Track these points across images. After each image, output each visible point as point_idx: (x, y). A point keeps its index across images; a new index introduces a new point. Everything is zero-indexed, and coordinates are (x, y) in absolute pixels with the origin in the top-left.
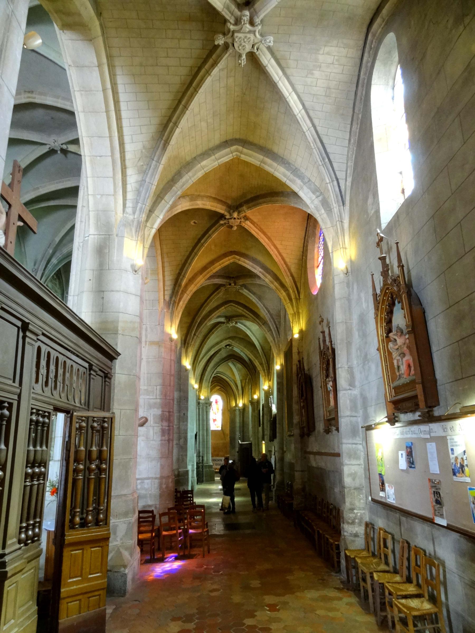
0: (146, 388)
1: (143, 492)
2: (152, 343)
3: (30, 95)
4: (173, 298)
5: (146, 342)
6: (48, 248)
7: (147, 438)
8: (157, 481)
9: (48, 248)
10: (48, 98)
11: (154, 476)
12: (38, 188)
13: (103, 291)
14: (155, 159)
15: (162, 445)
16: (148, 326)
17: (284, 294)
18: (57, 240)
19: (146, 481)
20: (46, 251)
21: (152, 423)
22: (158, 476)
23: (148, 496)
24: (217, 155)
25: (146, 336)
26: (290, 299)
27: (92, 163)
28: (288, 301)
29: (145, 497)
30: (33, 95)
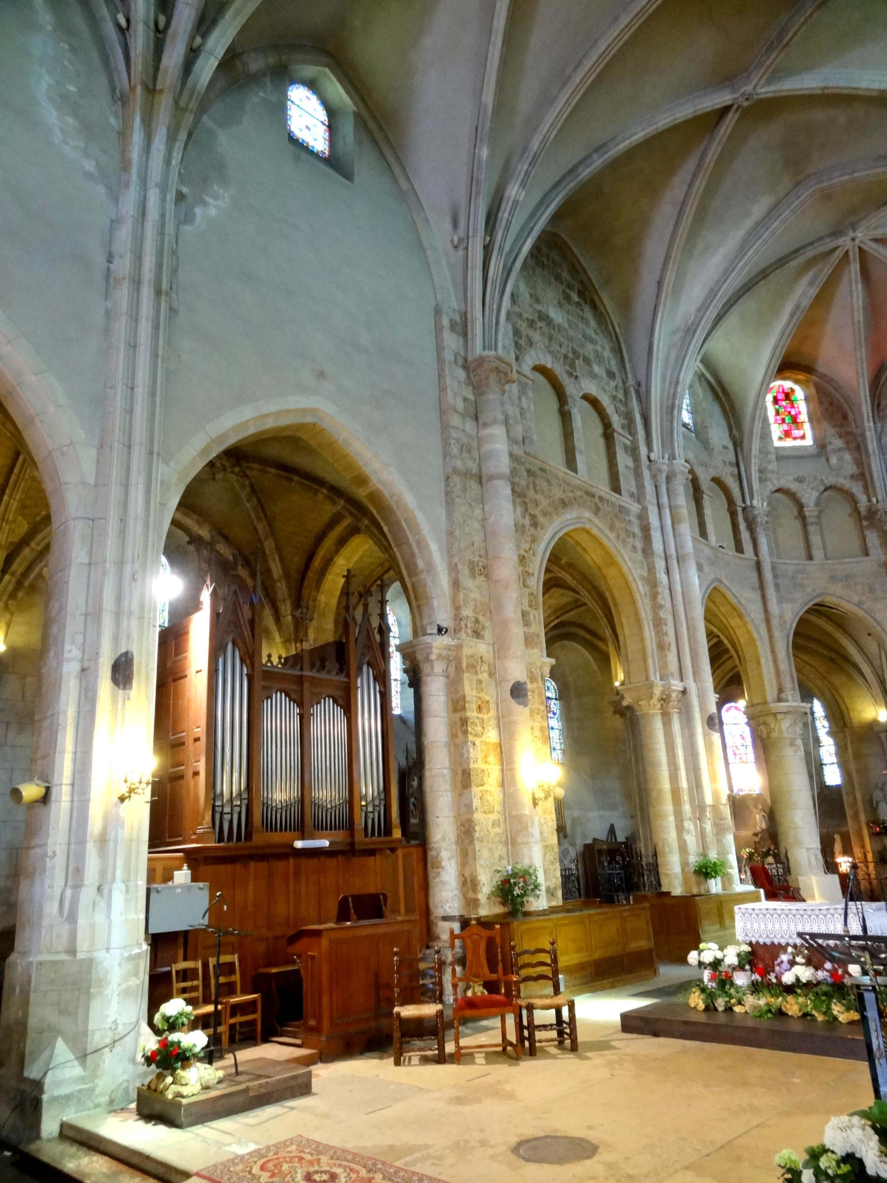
18: (489, 97)
20: (474, 157)
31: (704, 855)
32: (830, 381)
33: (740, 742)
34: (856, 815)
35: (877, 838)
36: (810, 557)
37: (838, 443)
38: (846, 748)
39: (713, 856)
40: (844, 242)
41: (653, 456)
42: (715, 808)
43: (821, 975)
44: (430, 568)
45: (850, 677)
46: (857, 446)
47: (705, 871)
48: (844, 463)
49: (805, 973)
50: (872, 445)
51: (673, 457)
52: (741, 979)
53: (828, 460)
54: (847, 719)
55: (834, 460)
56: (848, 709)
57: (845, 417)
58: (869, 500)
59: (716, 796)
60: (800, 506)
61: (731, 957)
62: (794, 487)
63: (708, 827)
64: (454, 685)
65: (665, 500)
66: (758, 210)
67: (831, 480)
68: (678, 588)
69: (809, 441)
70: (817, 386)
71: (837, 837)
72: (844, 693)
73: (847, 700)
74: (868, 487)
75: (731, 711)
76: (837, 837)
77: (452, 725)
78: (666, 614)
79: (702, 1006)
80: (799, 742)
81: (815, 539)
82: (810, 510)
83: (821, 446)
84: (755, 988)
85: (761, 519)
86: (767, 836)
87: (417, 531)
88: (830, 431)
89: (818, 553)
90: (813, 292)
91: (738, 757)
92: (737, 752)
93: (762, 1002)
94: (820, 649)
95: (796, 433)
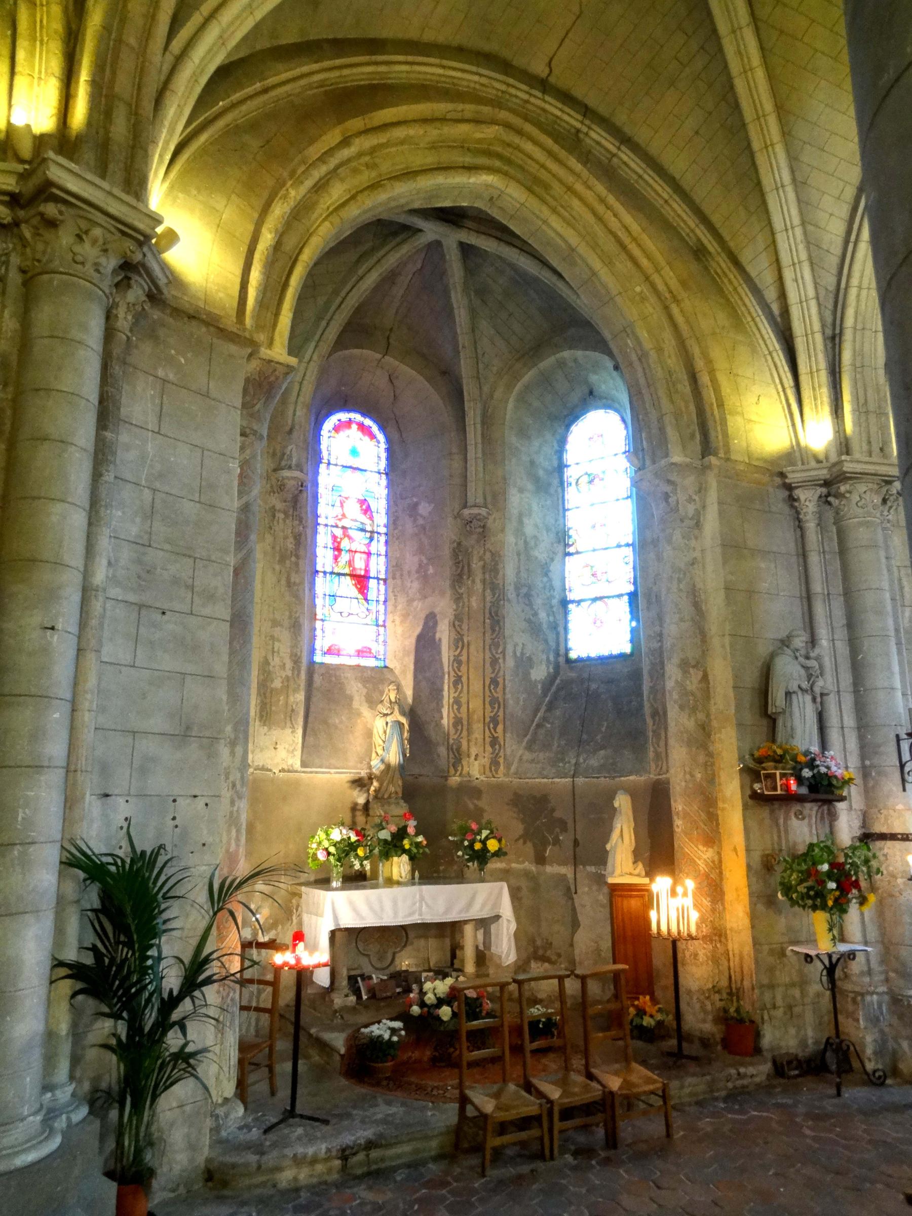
33: (353, 511)
34: (702, 738)
35: (764, 812)
38: (698, 525)
45: (737, 322)
54: (716, 436)
56: (721, 405)
71: (622, 802)
72: (716, 353)
73: (722, 378)
75: (343, 434)
76: (622, 802)
86: (395, 787)
91: (345, 557)
92: (345, 544)
94: (677, 210)
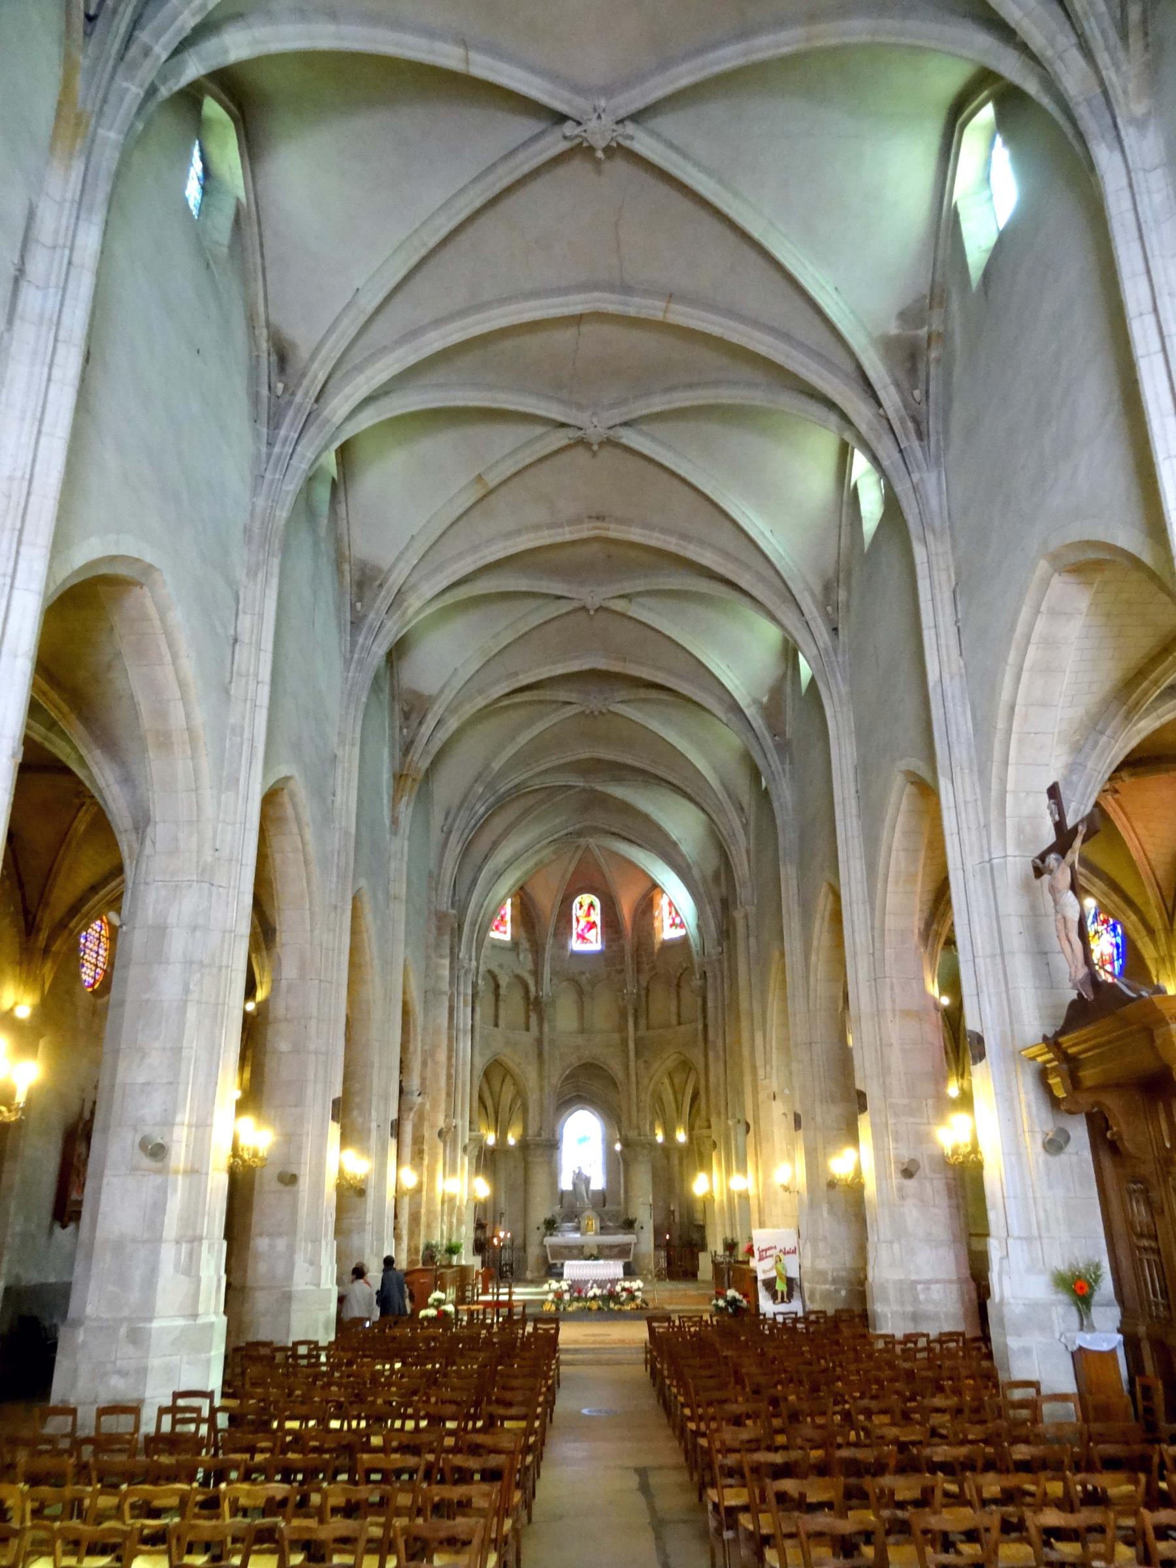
0: (906, 1101)
1: (930, 1308)
2: (906, 1013)
3: (599, 524)
4: (935, 927)
5: (894, 1010)
6: (476, 781)
7: (922, 1201)
8: (954, 1287)
9: (476, 781)
10: (633, 529)
11: (942, 1276)
12: (516, 674)
13: (1046, 953)
14: (1108, 732)
15: (951, 1216)
16: (895, 980)
17: (1134, 918)
18: (496, 766)
19: (935, 1287)
20: (471, 787)
21: (927, 1170)
22: (955, 1278)
23: (942, 1316)
24: (1159, 711)
25: (893, 1001)
26: (1151, 932)
27: (1020, 741)
28: (1144, 932)
29: (936, 1317)
30: (605, 525)
31: (450, 1240)
32: (531, 899)
36: (496, 1025)
37: (525, 945)
39: (454, 1240)
40: (582, 841)
41: (461, 955)
42: (459, 1208)
43: (605, 1292)
44: (416, 1051)
46: (537, 950)
47: (452, 1250)
48: (526, 958)
49: (598, 1292)
50: (547, 956)
51: (470, 960)
52: (567, 1297)
53: (518, 955)
55: (521, 957)
57: (533, 927)
58: (537, 991)
59: (461, 1201)
60: (497, 987)
61: (564, 1285)
62: (497, 971)
63: (455, 1221)
64: (417, 1127)
65: (462, 989)
66: (558, 821)
67: (519, 971)
68: (461, 1054)
69: (507, 937)
70: (522, 899)
74: (538, 983)
77: (413, 1152)
78: (453, 1072)
79: (554, 1308)
80: (474, 1161)
81: (502, 1012)
82: (502, 991)
83: (515, 944)
84: (578, 1299)
85: (481, 995)
87: (415, 1027)
88: (523, 935)
89: (501, 1022)
90: (554, 857)
93: (581, 1305)
95: (502, 928)
